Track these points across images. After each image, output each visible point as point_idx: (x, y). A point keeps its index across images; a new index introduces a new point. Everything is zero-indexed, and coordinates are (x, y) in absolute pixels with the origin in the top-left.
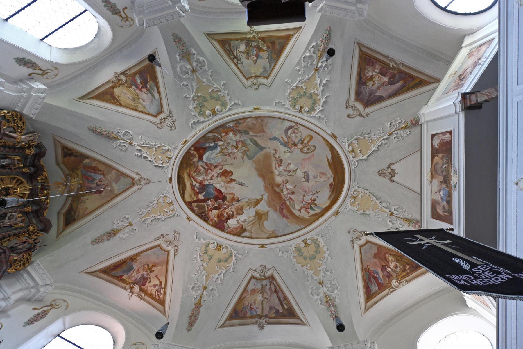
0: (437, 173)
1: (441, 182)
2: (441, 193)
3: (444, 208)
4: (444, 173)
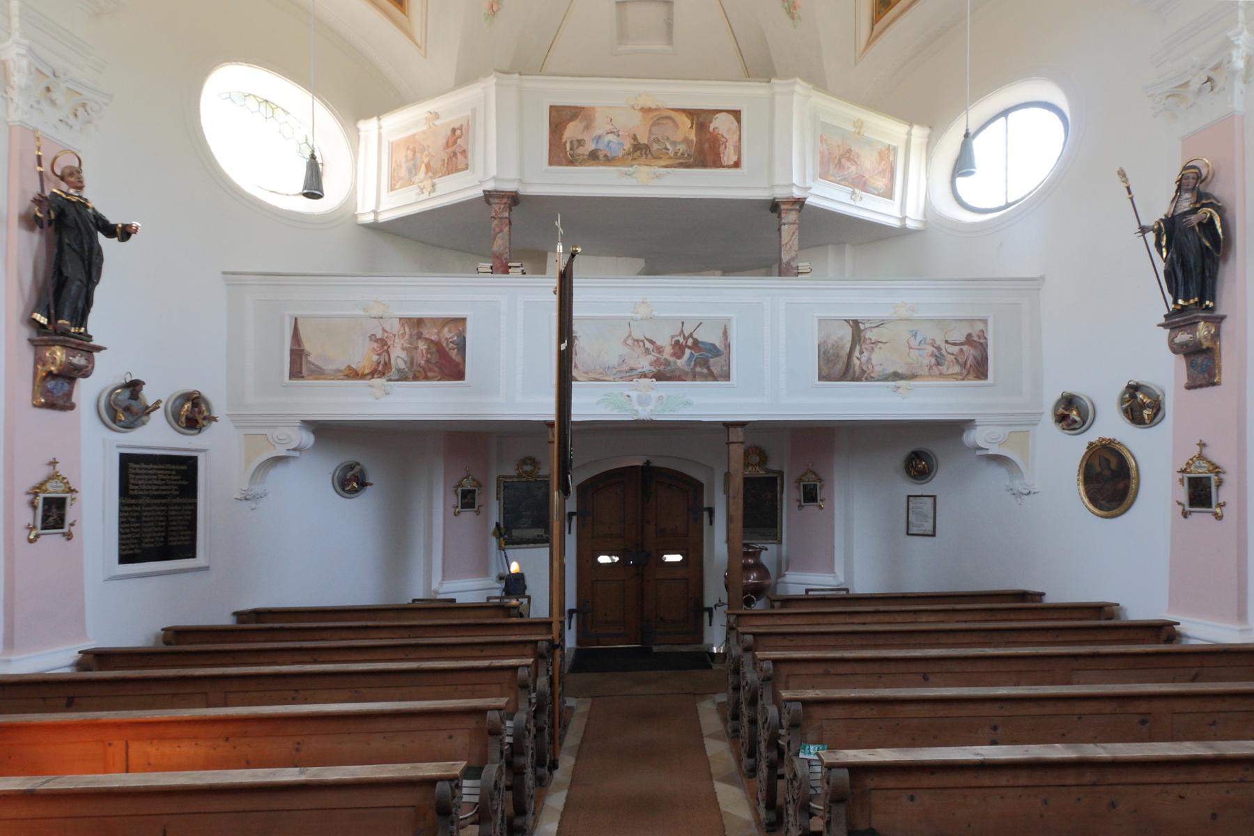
0: (654, 124)
1: (635, 138)
2: (611, 137)
3: (580, 143)
4: (655, 147)
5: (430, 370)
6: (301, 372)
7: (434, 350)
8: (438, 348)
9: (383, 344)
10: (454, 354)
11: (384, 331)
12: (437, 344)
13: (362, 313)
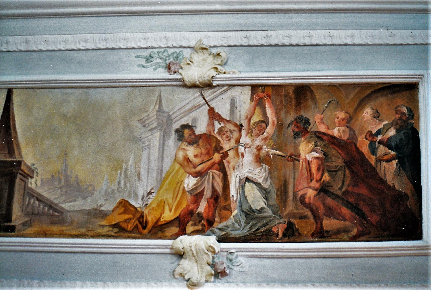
5: (330, 212)
6: (8, 217)
7: (338, 162)
8: (346, 156)
9: (211, 148)
10: (389, 171)
11: (214, 115)
12: (347, 146)
13: (162, 74)
